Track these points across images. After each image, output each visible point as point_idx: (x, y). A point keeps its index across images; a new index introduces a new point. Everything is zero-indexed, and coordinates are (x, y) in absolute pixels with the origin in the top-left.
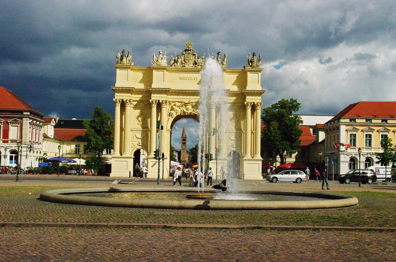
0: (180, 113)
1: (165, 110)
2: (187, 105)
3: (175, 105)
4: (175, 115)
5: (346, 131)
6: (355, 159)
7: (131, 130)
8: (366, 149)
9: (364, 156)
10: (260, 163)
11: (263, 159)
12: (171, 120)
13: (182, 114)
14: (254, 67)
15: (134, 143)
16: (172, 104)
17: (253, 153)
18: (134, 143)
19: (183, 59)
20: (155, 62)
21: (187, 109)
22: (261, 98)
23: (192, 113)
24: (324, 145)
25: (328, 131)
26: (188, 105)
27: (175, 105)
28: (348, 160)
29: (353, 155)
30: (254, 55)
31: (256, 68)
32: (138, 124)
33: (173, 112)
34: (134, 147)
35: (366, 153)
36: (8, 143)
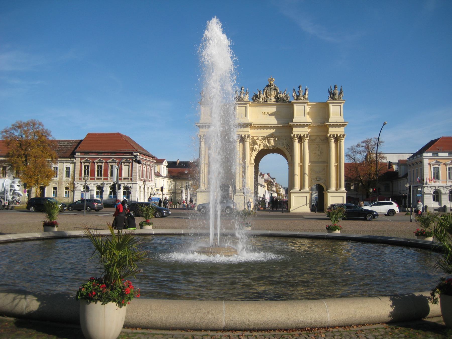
5: (429, 164)
6: (439, 192)
8: (449, 181)
9: (432, 188)
10: (345, 196)
11: (347, 192)
12: (255, 154)
13: (265, 149)
14: (336, 99)
17: (338, 186)
19: (264, 95)
22: (343, 130)
24: (407, 179)
25: (418, 164)
28: (432, 192)
29: (437, 188)
30: (335, 87)
31: (338, 100)
33: (256, 146)
35: (449, 186)
36: (94, 180)
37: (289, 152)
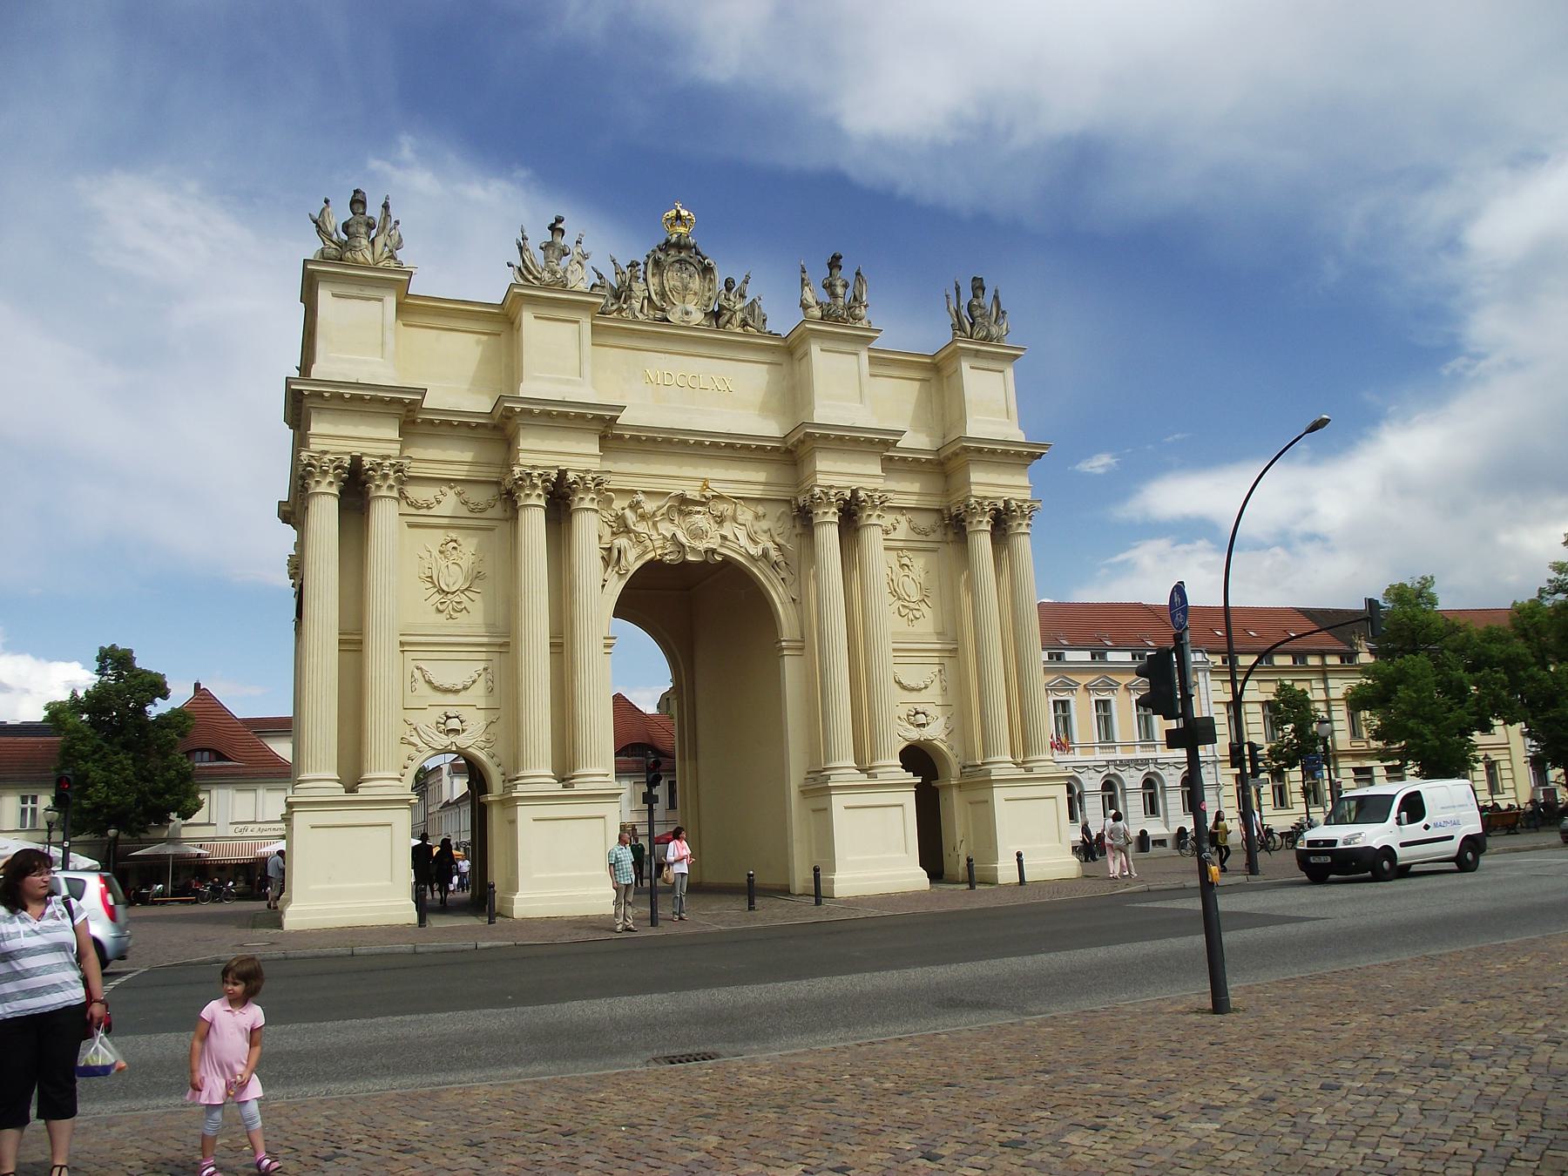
0: (659, 552)
1: (589, 529)
2: (690, 513)
3: (635, 506)
4: (633, 562)
7: (402, 644)
15: (413, 717)
16: (619, 504)
18: (413, 717)
20: (530, 273)
21: (698, 534)
23: (714, 551)
26: (699, 508)
27: (635, 506)
32: (439, 611)
33: (622, 542)
34: (415, 740)
37: (782, 579)
